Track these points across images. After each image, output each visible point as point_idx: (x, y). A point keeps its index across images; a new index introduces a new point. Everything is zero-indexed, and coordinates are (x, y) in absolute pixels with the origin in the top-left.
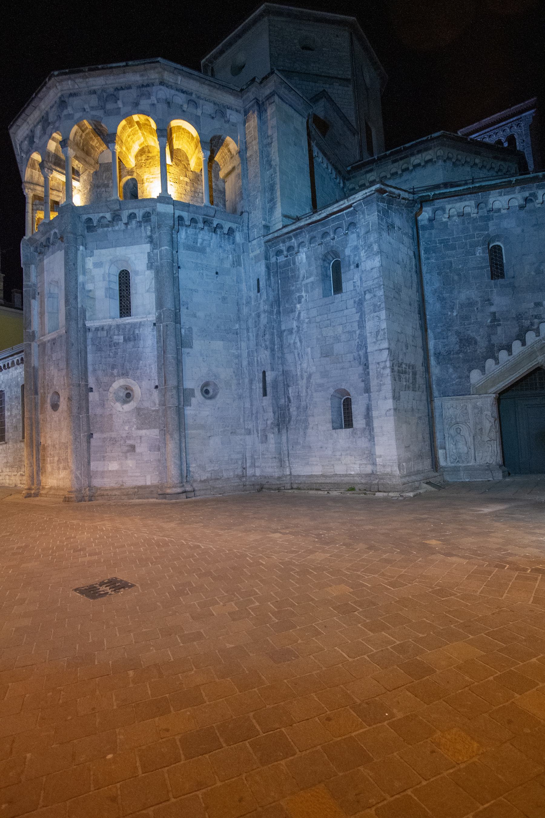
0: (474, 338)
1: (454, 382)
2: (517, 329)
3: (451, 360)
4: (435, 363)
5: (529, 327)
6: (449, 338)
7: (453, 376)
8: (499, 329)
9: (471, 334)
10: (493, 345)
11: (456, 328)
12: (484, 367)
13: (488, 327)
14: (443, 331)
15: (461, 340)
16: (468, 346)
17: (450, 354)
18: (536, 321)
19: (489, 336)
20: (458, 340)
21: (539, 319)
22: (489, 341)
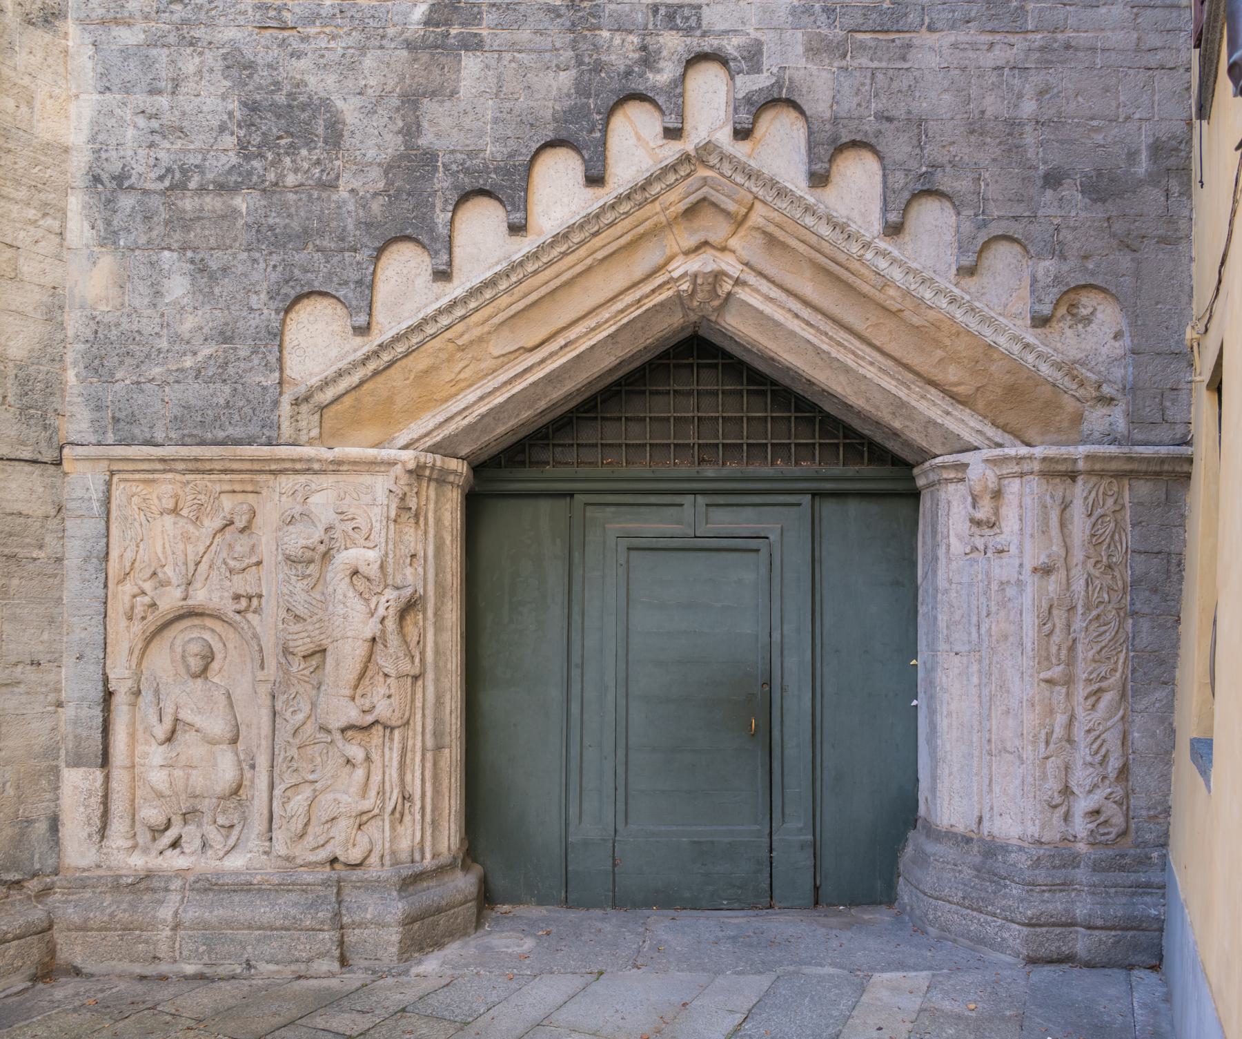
0: (326, 103)
1: (188, 362)
2: (566, 79)
3: (187, 228)
4: (88, 234)
5: (628, 73)
6: (188, 87)
7: (188, 324)
8: (471, 64)
9: (312, 80)
10: (429, 158)
11: (231, 33)
12: (367, 286)
13: (410, 46)
14: (155, 42)
15: (252, 107)
16: (292, 150)
17: (182, 186)
18: (672, 43)
19: (411, 101)
20: (234, 105)
21: (688, 31)
22: (411, 131)
